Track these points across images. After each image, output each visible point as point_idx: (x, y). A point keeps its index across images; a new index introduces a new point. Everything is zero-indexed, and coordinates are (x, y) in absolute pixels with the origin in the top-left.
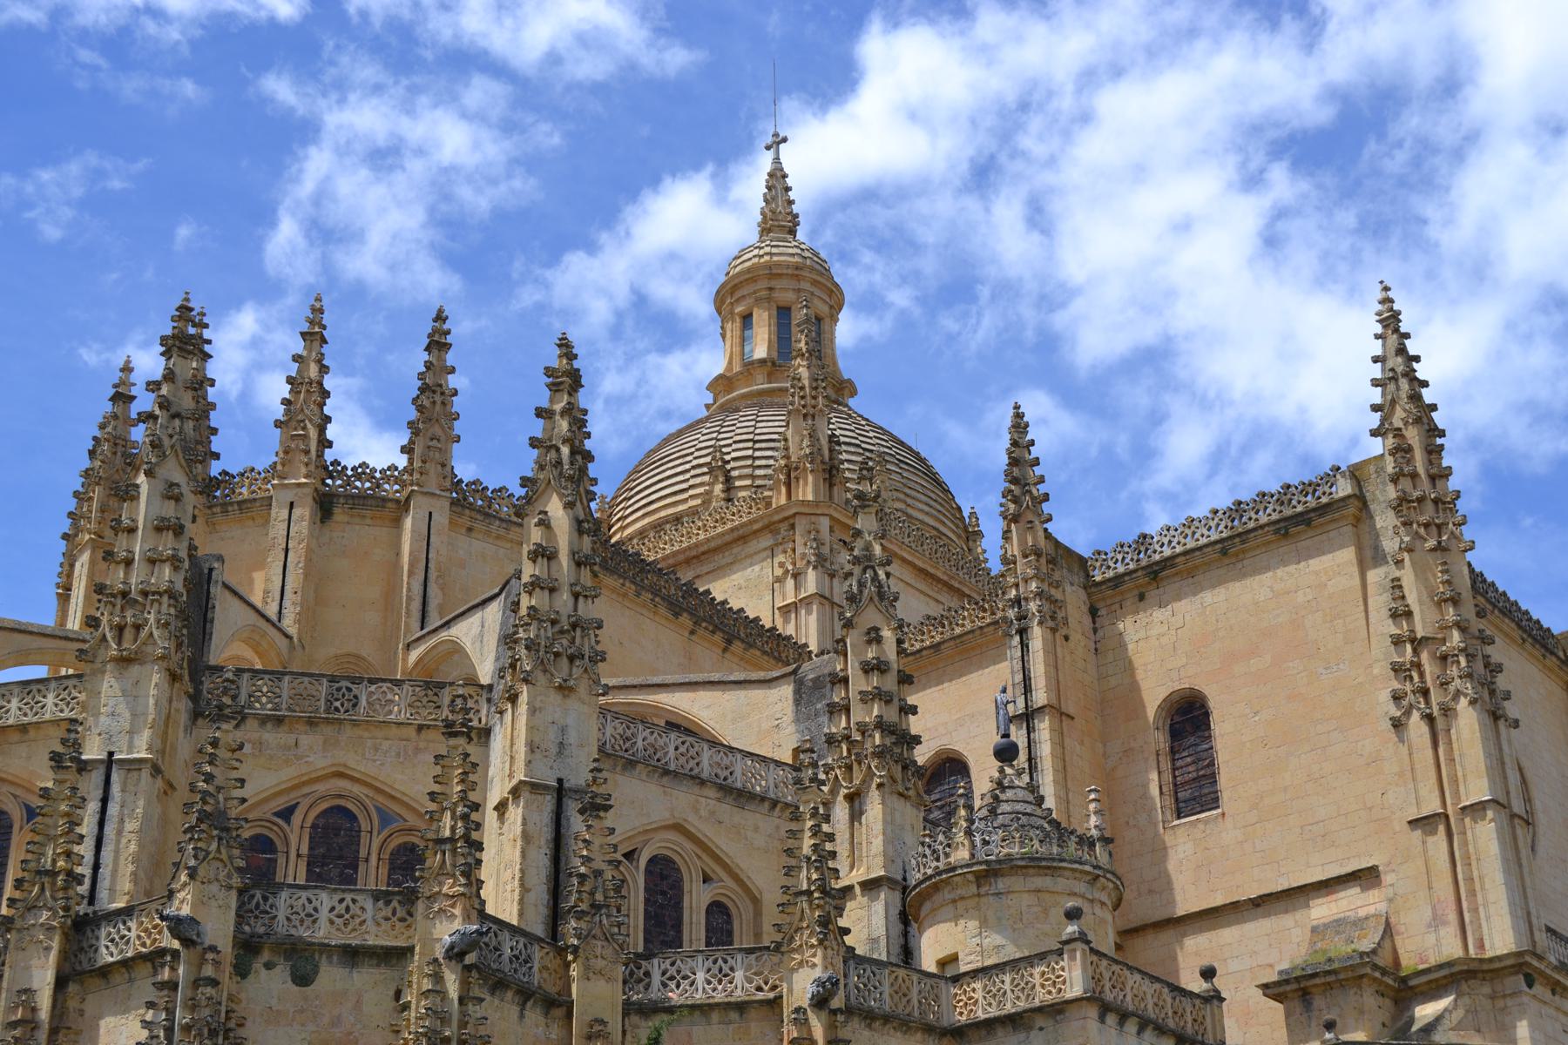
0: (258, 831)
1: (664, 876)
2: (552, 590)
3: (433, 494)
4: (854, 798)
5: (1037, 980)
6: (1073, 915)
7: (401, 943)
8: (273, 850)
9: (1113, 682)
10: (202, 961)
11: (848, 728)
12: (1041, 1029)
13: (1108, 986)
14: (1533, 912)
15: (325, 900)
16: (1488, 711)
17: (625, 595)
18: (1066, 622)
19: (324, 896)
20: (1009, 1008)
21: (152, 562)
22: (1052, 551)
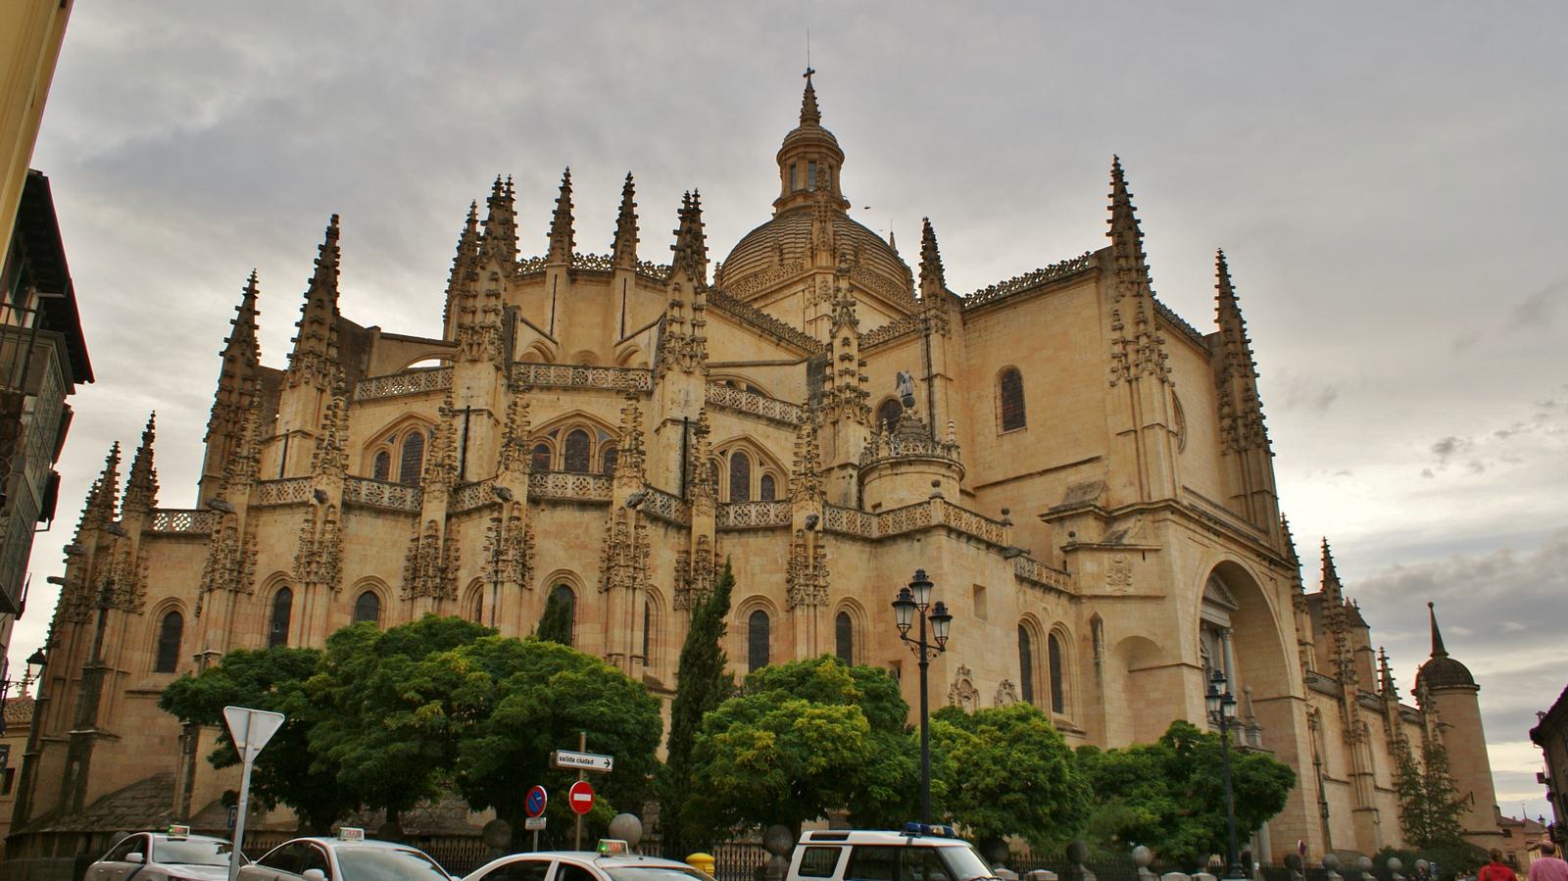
0: (537, 444)
1: (740, 464)
2: (682, 323)
3: (627, 270)
4: (835, 423)
5: (918, 516)
6: (936, 484)
7: (606, 499)
8: (549, 453)
9: (973, 362)
10: (513, 509)
11: (833, 388)
12: (919, 540)
13: (953, 518)
14: (1176, 479)
15: (571, 479)
16: (1159, 379)
17: (726, 319)
18: (949, 332)
19: (570, 477)
20: (904, 529)
21: (485, 312)
22: (944, 295)
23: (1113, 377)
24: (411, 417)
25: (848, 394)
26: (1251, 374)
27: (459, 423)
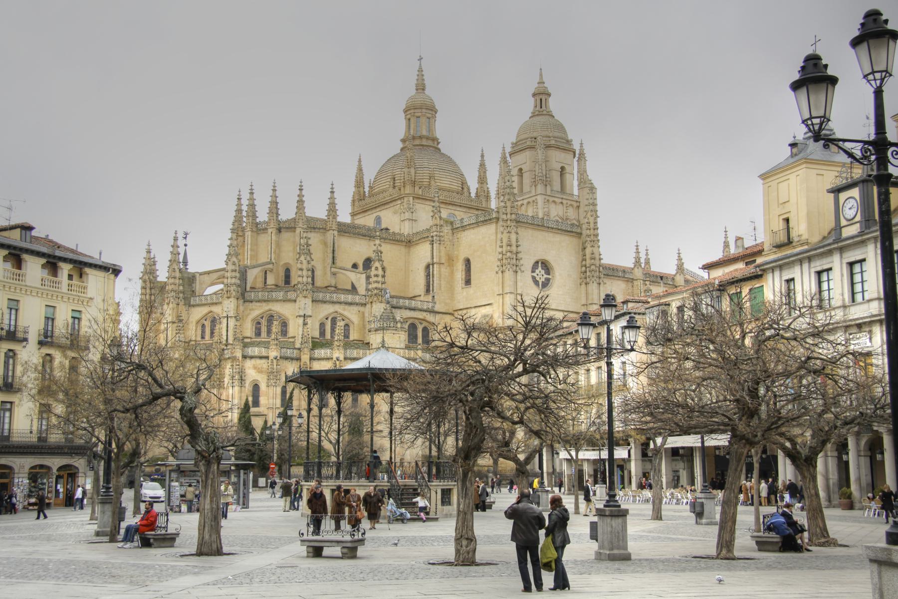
1: (334, 321)
4: (371, 303)
23: (497, 269)
24: (211, 312)
25: (376, 291)
26: (596, 246)
27: (225, 321)
